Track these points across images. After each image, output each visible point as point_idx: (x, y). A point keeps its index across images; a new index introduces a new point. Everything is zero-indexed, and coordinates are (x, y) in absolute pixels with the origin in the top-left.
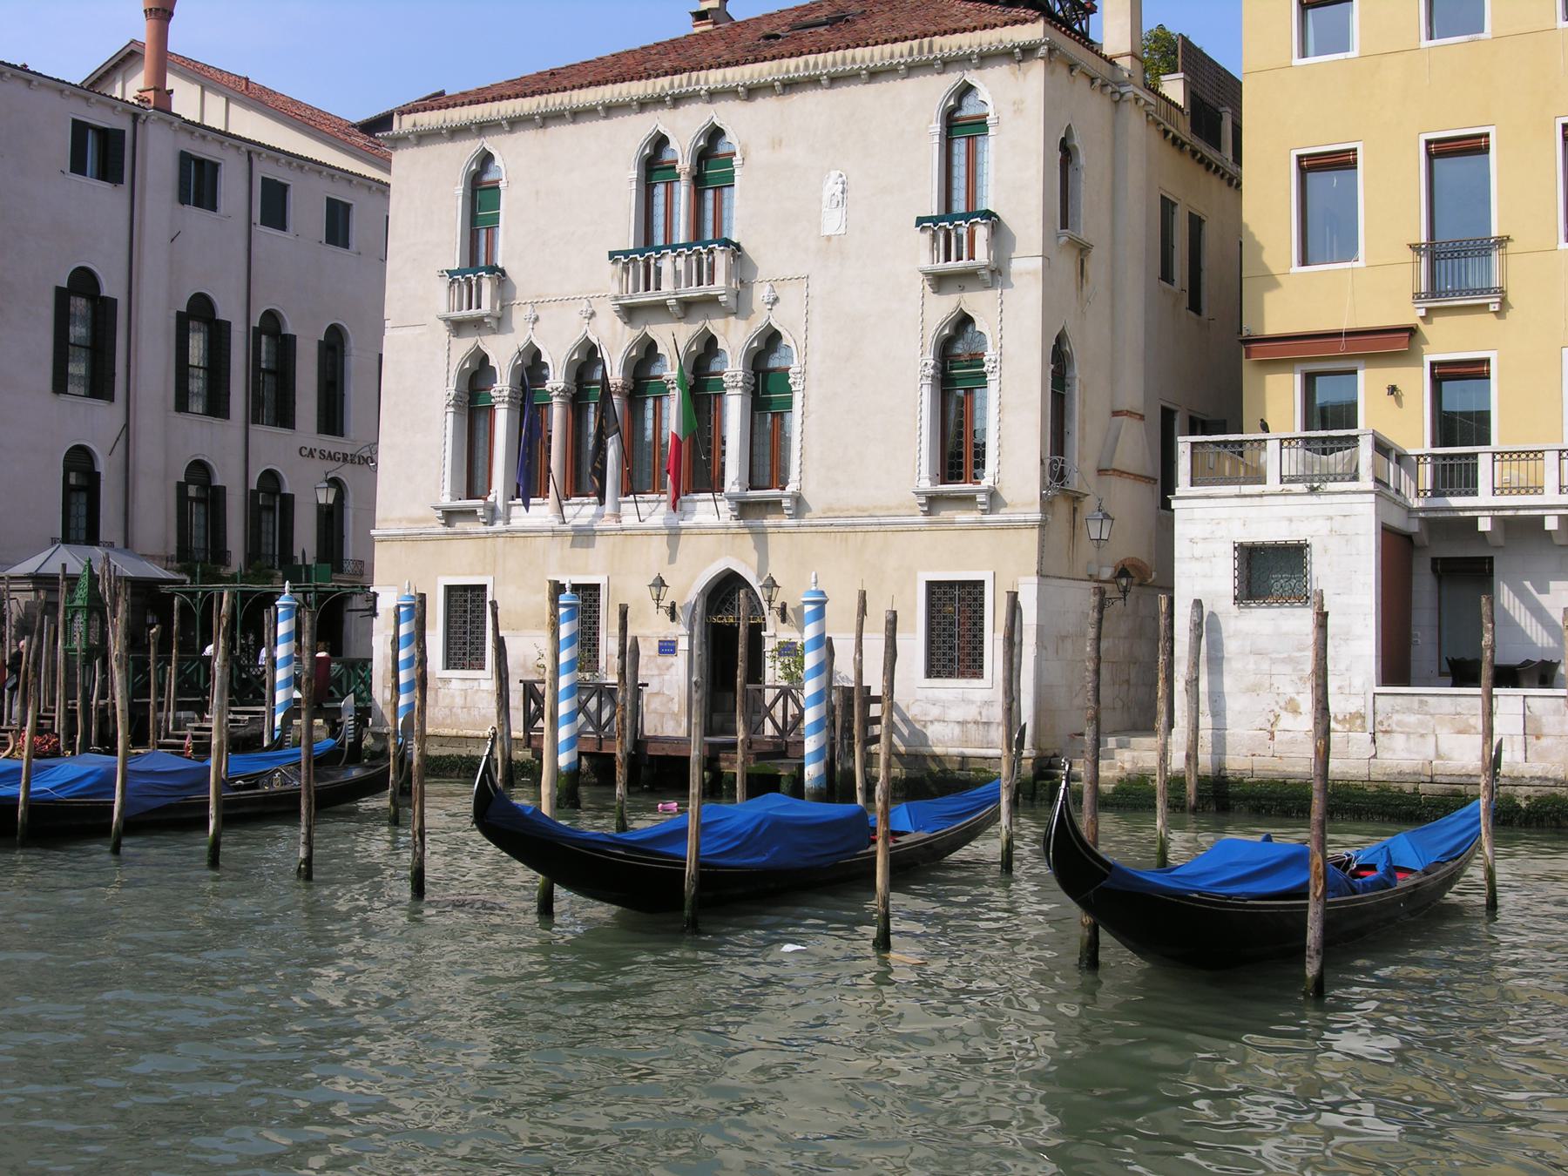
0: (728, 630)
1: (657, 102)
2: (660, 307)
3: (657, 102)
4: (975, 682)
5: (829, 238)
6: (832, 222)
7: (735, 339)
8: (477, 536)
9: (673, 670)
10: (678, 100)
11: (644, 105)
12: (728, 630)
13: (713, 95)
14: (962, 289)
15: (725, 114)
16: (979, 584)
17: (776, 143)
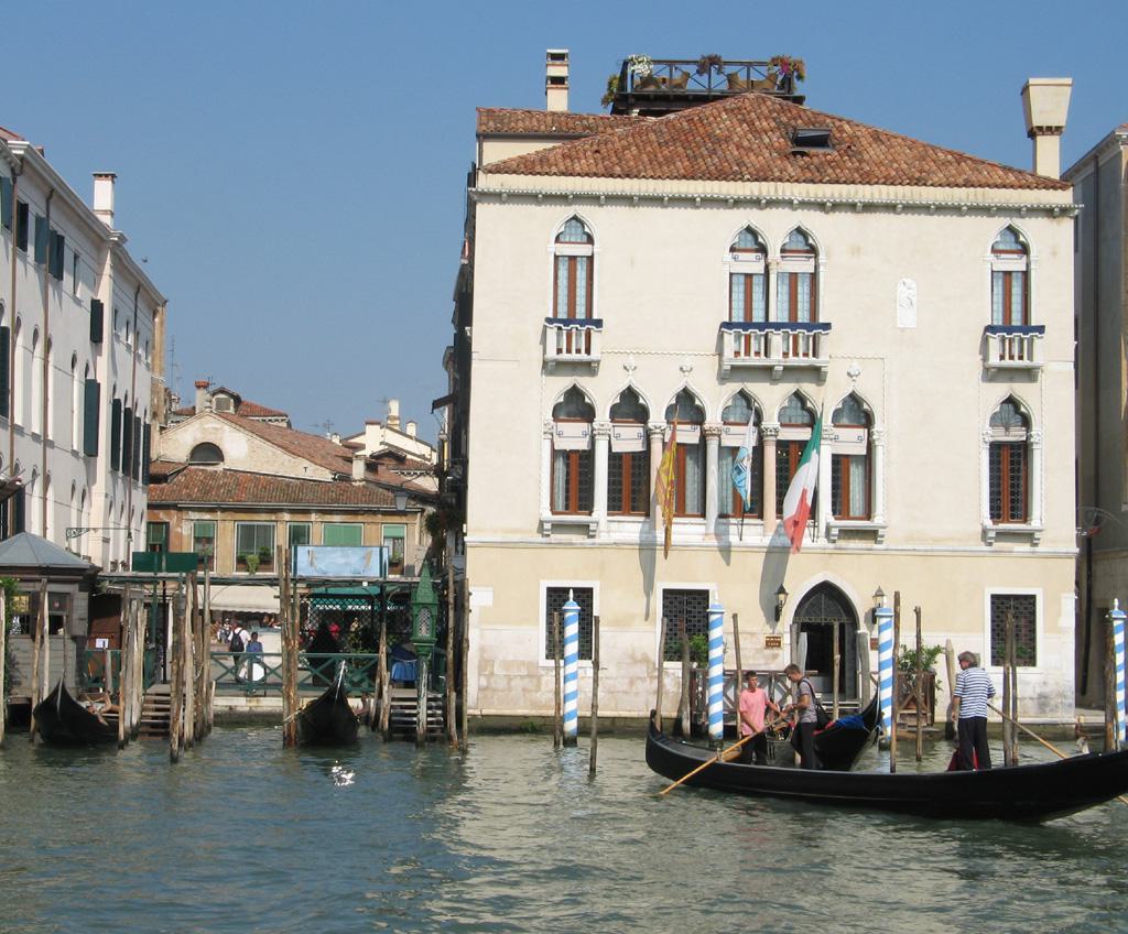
0: (828, 627)
1: (755, 203)
2: (769, 369)
3: (755, 203)
4: (1031, 669)
5: (903, 330)
6: (907, 318)
7: (826, 399)
8: (583, 547)
9: (780, 658)
10: (771, 203)
11: (738, 203)
12: (828, 627)
13: (804, 204)
14: (1011, 380)
15: (812, 221)
16: (1033, 597)
17: (856, 251)
